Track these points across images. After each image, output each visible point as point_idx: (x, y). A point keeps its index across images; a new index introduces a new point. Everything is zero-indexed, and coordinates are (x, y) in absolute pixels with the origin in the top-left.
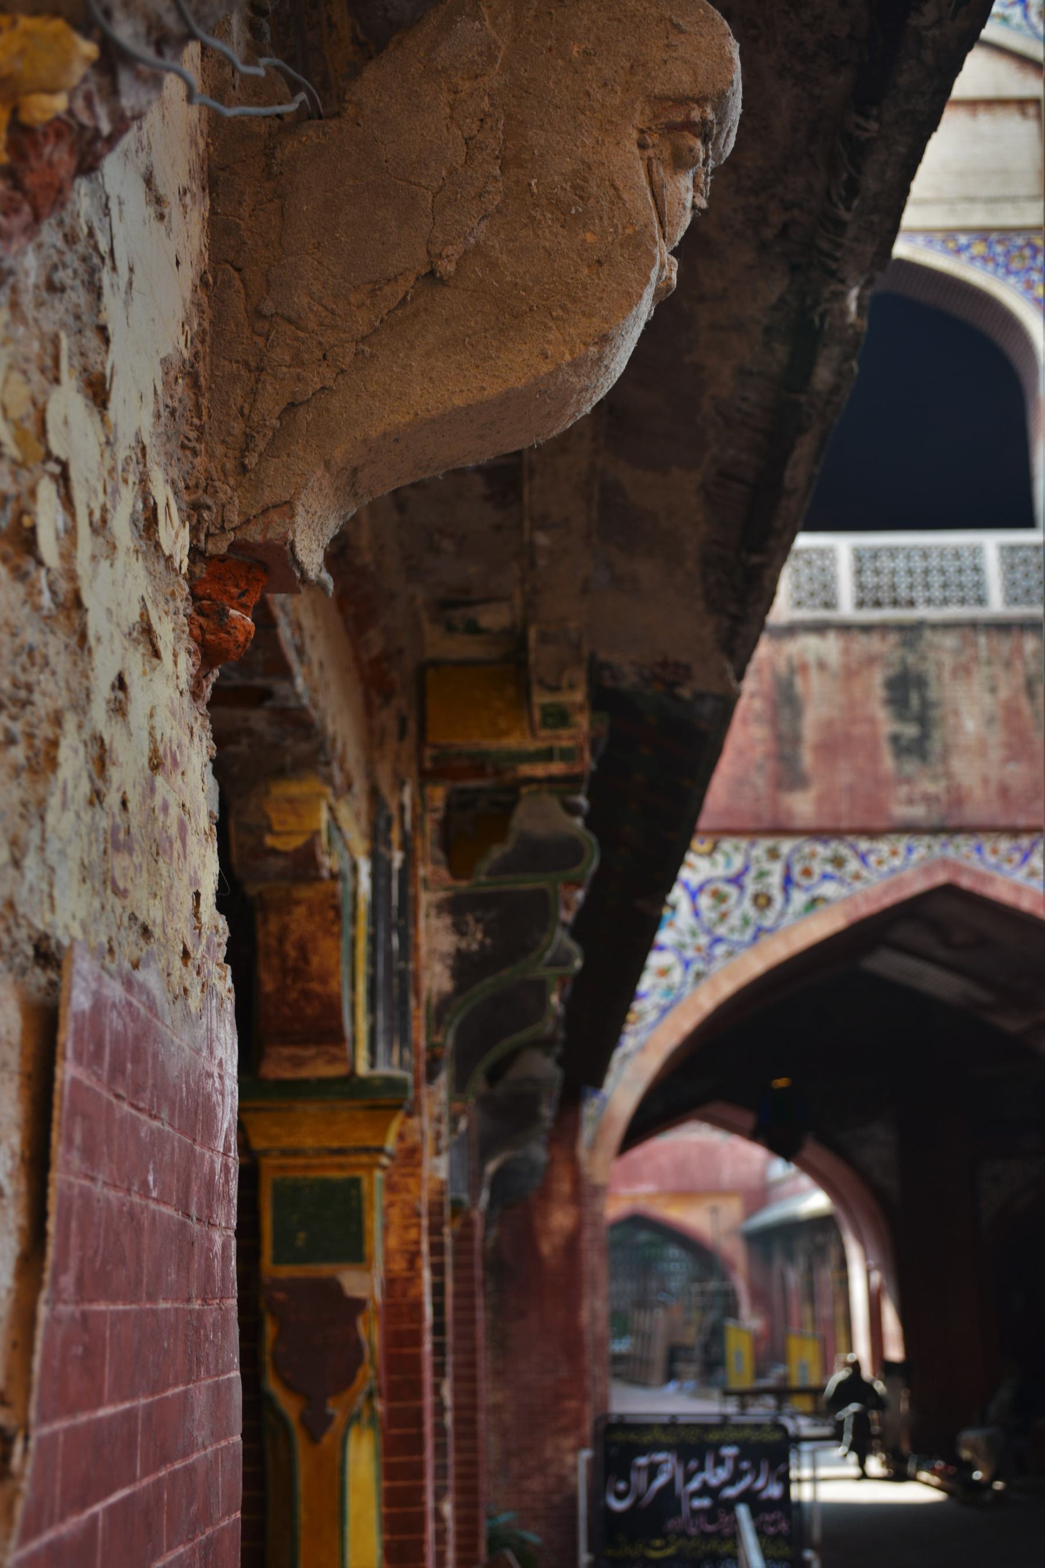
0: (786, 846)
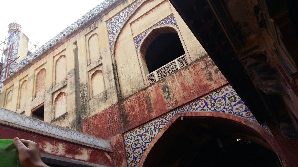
0: (153, 122)
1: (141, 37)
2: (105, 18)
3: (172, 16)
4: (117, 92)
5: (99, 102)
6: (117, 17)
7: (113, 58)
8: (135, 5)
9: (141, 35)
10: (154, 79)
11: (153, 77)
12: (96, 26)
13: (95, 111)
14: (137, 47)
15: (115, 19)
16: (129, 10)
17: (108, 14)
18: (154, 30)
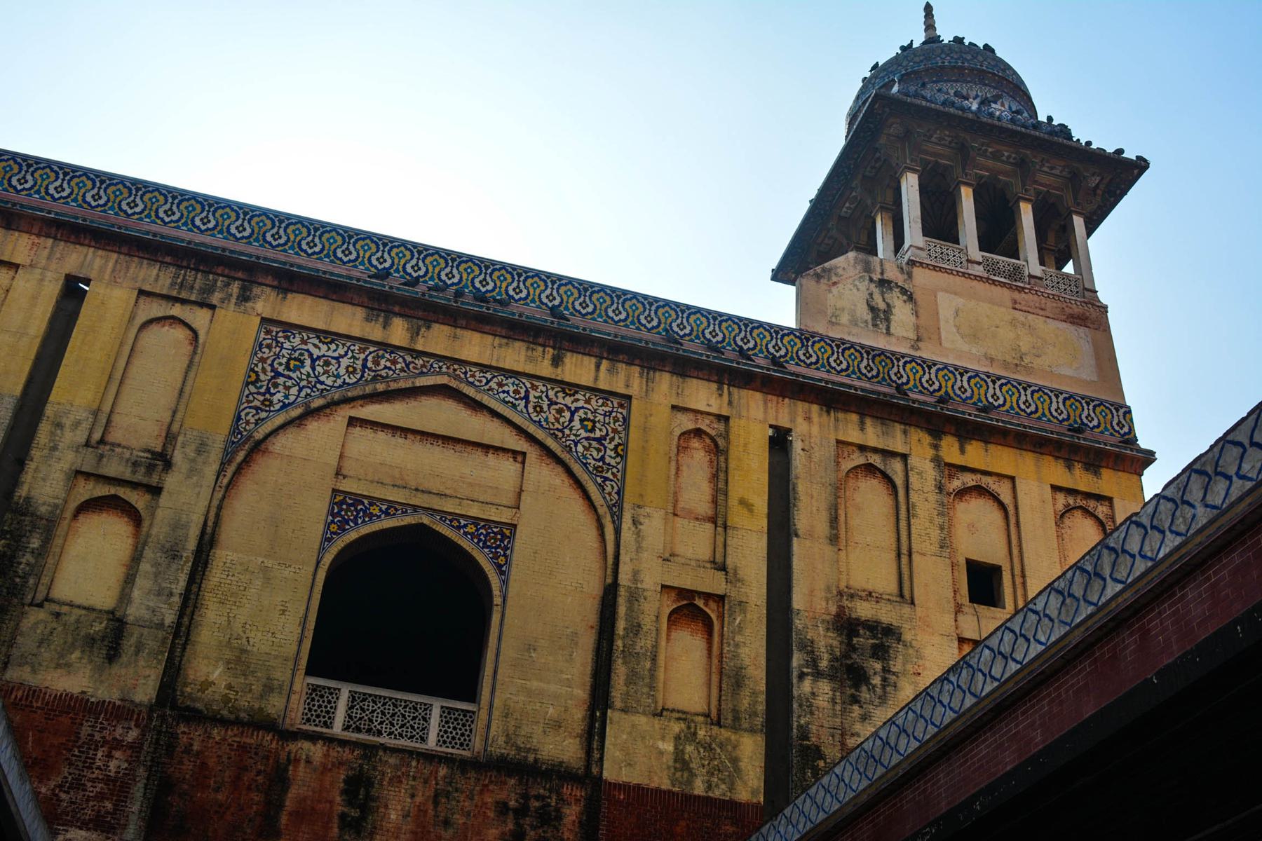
1: (365, 512)
2: (265, 303)
3: (507, 532)
4: (170, 659)
5: (73, 646)
6: (316, 342)
7: (215, 503)
8: (407, 366)
9: (366, 502)
10: (328, 712)
11: (329, 702)
12: (215, 299)
13: (34, 671)
14: (329, 540)
15: (304, 342)
16: (376, 363)
17: (289, 296)
18: (422, 525)
